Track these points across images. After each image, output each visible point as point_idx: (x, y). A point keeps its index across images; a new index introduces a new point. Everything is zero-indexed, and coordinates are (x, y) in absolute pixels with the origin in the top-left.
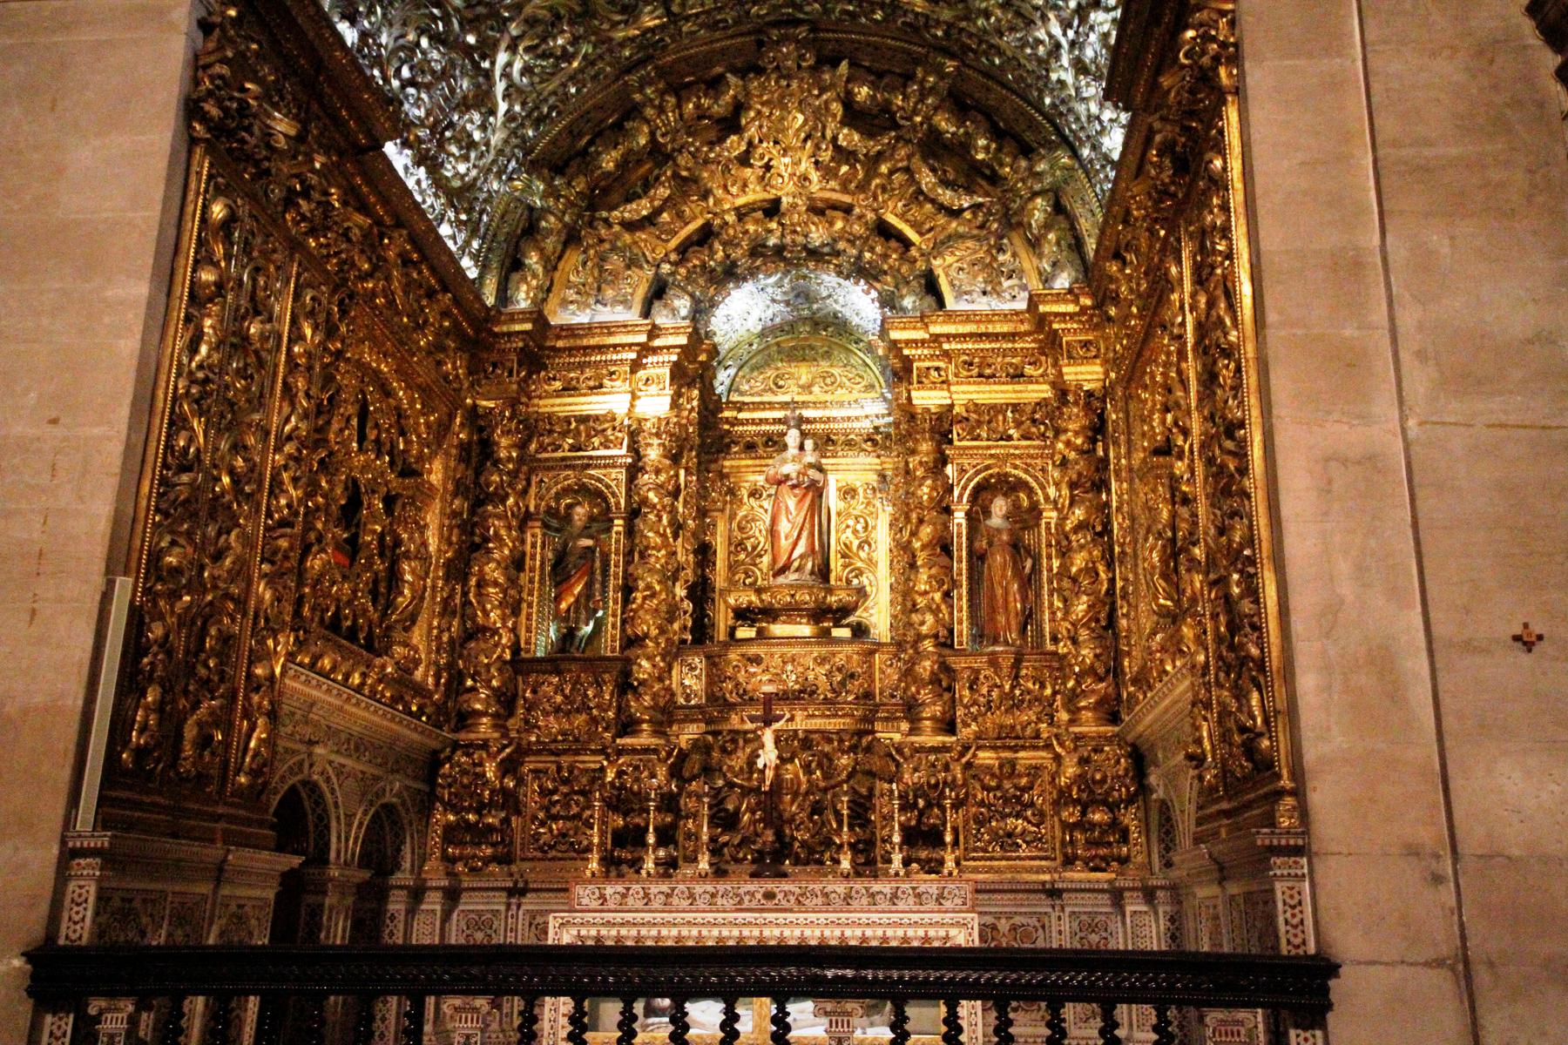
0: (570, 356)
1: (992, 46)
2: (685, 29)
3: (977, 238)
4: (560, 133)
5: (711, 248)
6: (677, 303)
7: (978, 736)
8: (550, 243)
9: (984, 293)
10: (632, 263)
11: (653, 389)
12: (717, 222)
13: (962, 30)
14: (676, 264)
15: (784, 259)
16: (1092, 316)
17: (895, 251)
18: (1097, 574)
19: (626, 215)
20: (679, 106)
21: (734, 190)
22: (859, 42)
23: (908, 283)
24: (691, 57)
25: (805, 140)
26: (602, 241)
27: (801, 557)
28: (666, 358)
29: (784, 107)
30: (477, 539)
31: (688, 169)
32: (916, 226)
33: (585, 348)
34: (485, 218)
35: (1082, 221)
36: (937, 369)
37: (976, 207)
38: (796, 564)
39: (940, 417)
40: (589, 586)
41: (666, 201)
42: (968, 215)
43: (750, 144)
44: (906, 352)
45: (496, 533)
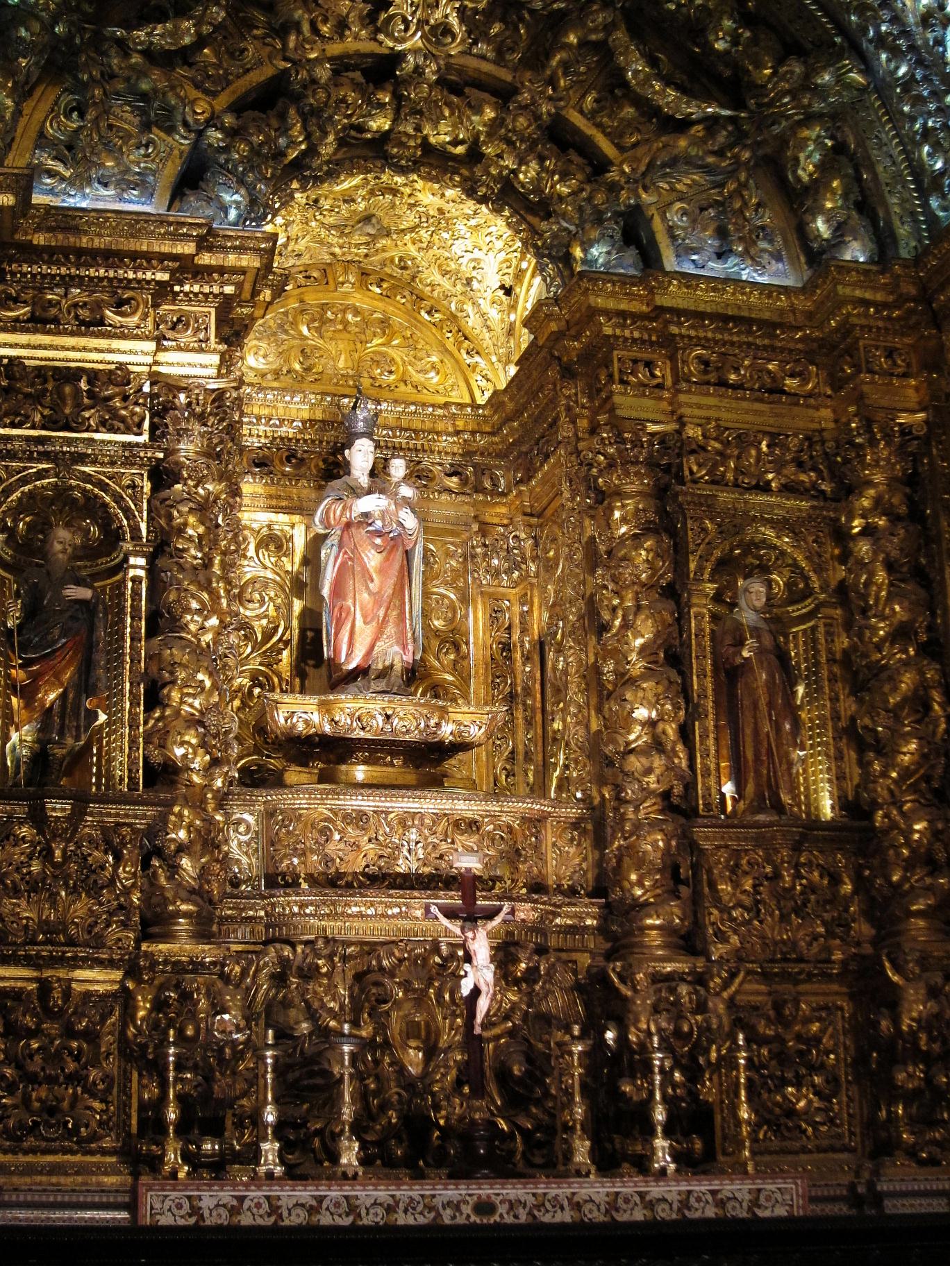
0: (50, 263)
3: (707, 169)
5: (283, 116)
6: (227, 198)
7: (739, 956)
9: (720, 255)
11: (186, 338)
12: (303, 75)
14: (233, 134)
16: (911, 312)
17: (582, 169)
18: (928, 708)
19: (155, 40)
21: (325, 29)
23: (599, 220)
26: (113, 76)
28: (216, 290)
32: (615, 137)
33: (80, 252)
35: (880, 169)
37: (712, 123)
41: (218, 28)
42: (698, 130)
44: (608, 330)
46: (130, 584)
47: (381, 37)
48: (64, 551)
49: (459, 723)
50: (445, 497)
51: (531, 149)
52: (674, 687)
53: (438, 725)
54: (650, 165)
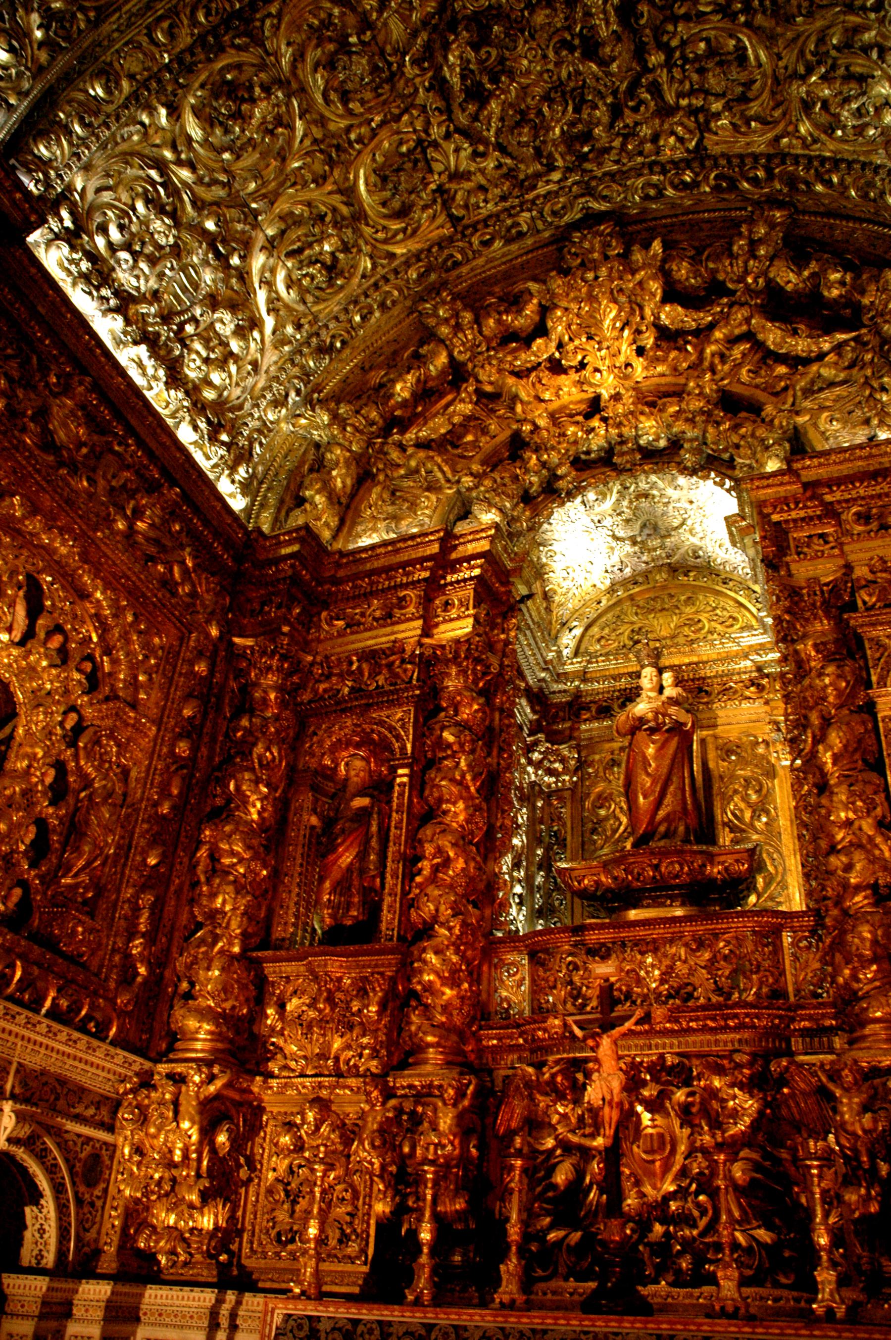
1: (823, 160)
2: (475, 240)
4: (351, 371)
8: (340, 479)
10: (432, 487)
12: (527, 428)
13: (783, 157)
14: (479, 477)
15: (614, 467)
20: (477, 321)
22: (672, 225)
23: (767, 448)
24: (489, 277)
25: (622, 329)
27: (667, 818)
29: (592, 298)
30: (219, 802)
31: (491, 383)
32: (767, 389)
34: (257, 449)
36: (822, 536)
37: (838, 348)
38: (662, 829)
39: (835, 588)
40: (362, 856)
41: (468, 418)
43: (560, 346)
44: (775, 518)
45: (238, 788)
46: (397, 788)
47: (585, 388)
48: (357, 775)
49: (722, 863)
50: (745, 705)
51: (707, 422)
52: (869, 790)
53: (704, 866)
54: (794, 396)
